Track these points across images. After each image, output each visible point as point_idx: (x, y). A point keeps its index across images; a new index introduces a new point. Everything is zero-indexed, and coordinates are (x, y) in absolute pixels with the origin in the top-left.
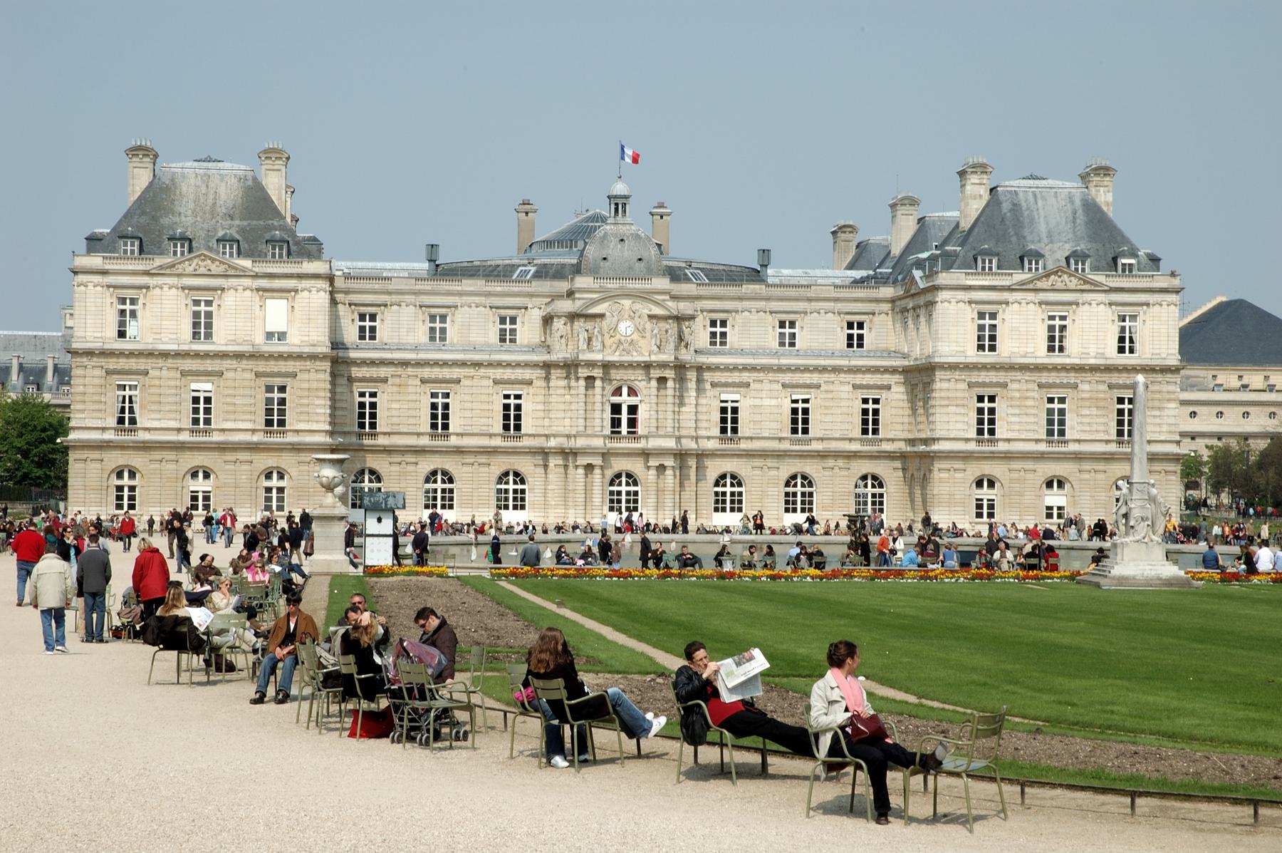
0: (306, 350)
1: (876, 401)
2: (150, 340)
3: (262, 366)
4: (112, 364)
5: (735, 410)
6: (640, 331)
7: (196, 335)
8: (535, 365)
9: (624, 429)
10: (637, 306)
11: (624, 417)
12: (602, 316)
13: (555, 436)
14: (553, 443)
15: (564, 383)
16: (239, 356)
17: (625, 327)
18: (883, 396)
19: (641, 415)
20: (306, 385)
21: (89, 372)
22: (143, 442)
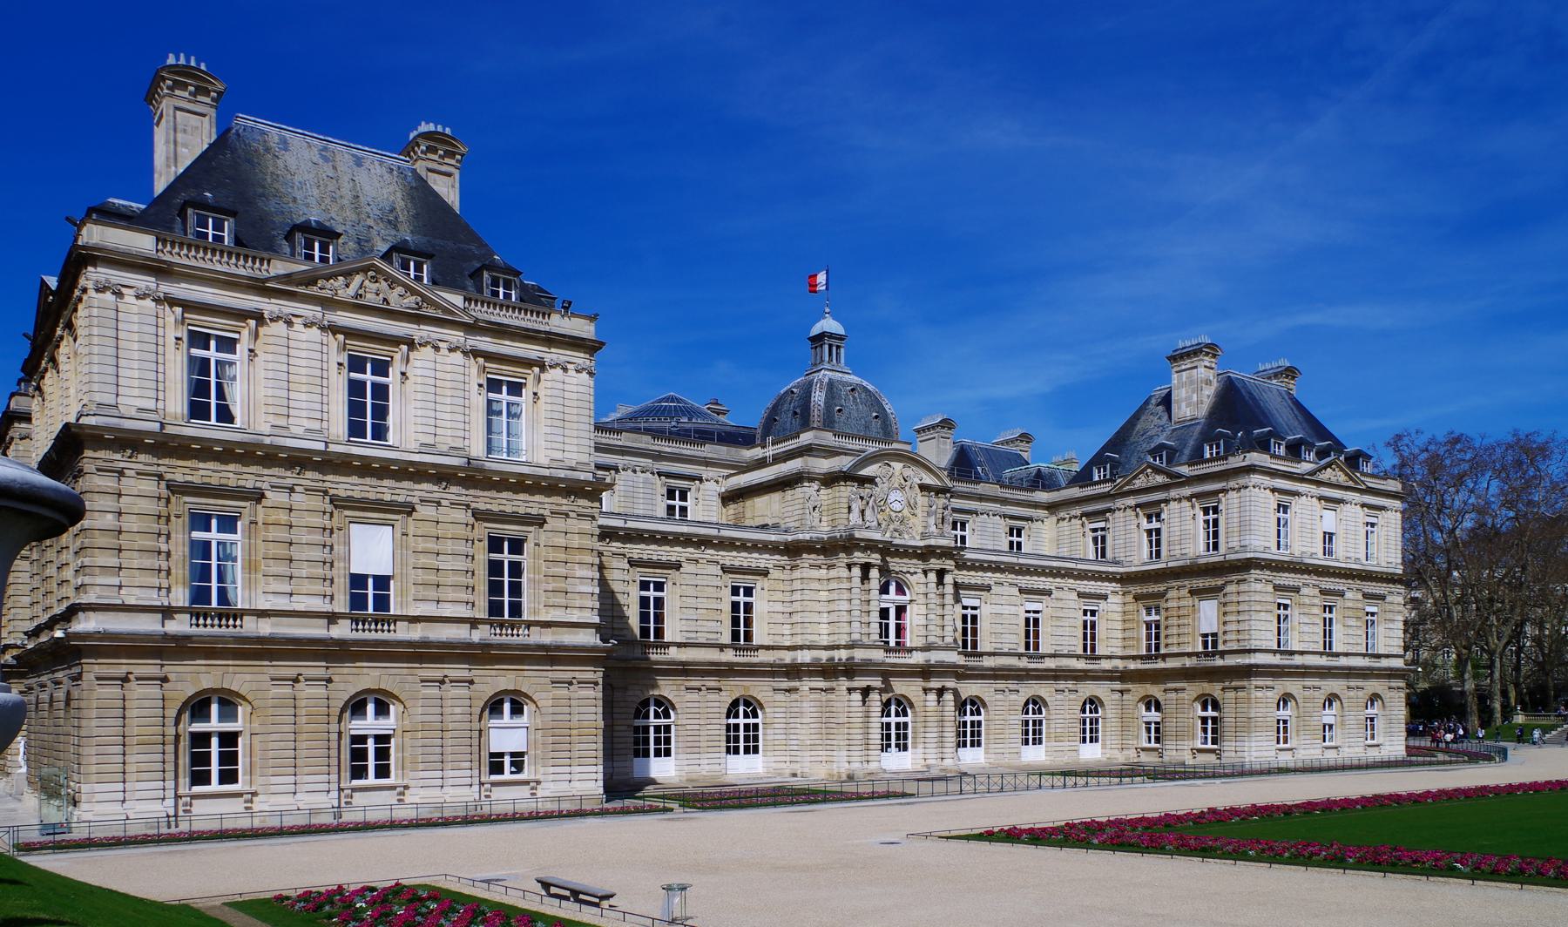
0: (562, 474)
1: (1093, 613)
2: (266, 429)
3: (487, 500)
4: (182, 471)
5: (974, 618)
6: (912, 506)
7: (356, 430)
8: (773, 548)
9: (892, 641)
10: (908, 472)
11: (892, 622)
12: (871, 480)
13: (810, 647)
14: (805, 657)
15: (815, 573)
16: (443, 476)
17: (897, 500)
18: (1103, 605)
19: (913, 618)
20: (560, 541)
21: (130, 484)
22: (260, 640)
